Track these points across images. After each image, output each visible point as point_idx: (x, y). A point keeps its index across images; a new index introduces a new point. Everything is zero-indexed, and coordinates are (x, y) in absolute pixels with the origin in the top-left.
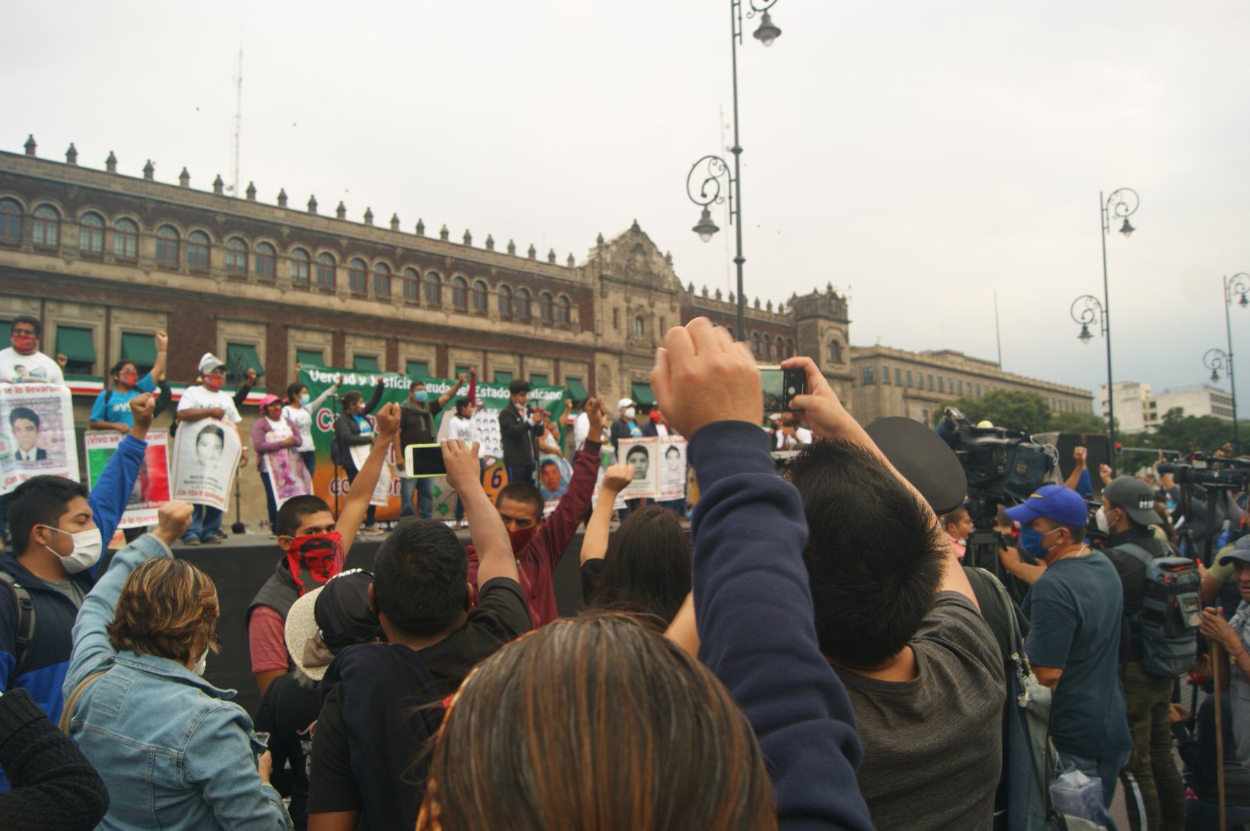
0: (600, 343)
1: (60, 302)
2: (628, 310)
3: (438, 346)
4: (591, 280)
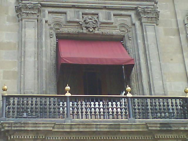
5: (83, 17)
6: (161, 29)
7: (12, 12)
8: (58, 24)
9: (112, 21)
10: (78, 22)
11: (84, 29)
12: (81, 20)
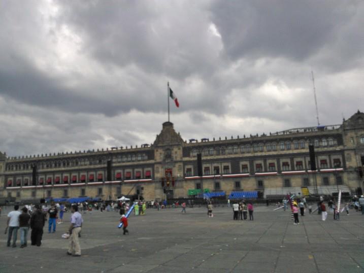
0: (346, 148)
1: (214, 163)
2: (357, 137)
3: (290, 158)
4: (340, 132)
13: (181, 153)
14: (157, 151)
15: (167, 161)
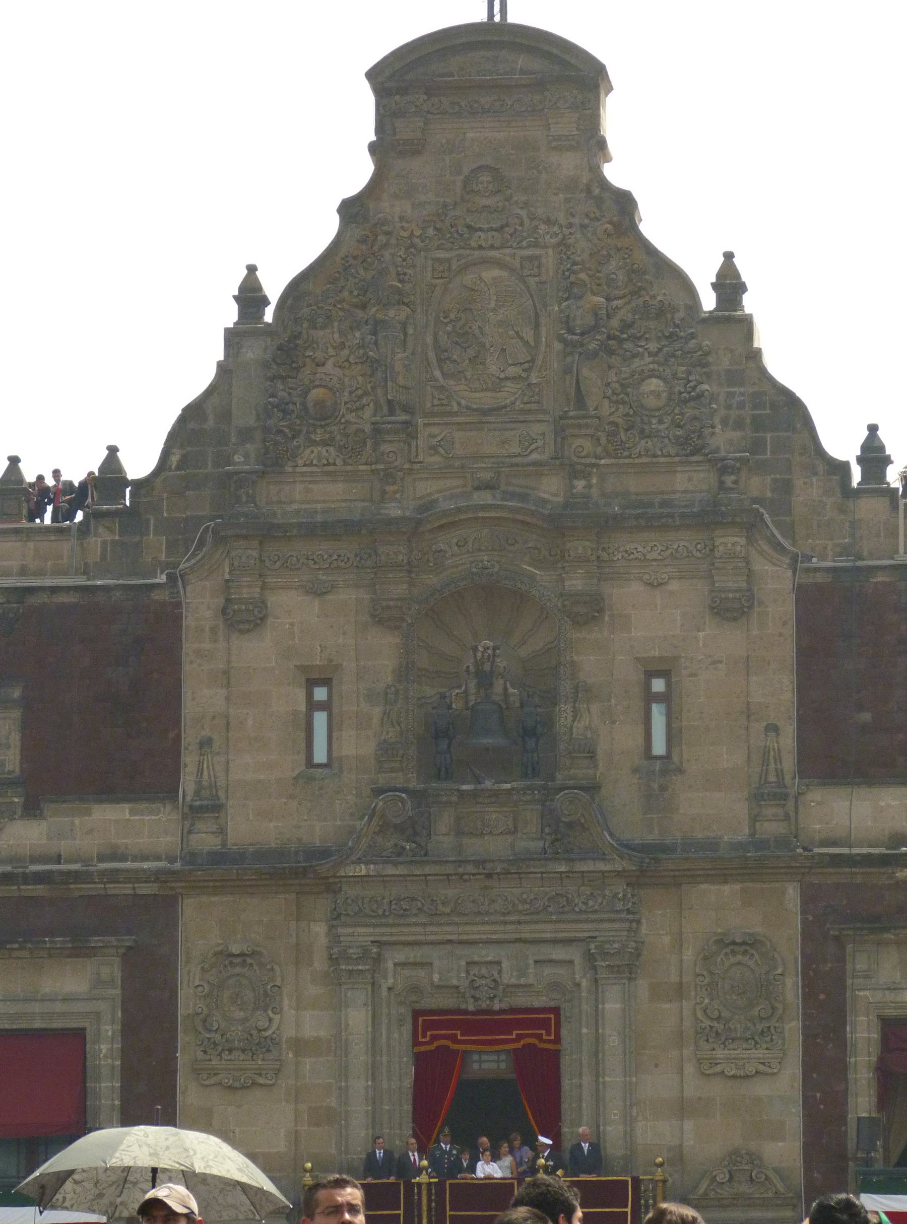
5: (468, 972)
6: (643, 986)
7: (320, 963)
8: (415, 989)
9: (531, 980)
10: (457, 987)
11: (471, 1000)
12: (464, 984)
13: (777, 690)
14: (244, 618)
15: (443, 838)
